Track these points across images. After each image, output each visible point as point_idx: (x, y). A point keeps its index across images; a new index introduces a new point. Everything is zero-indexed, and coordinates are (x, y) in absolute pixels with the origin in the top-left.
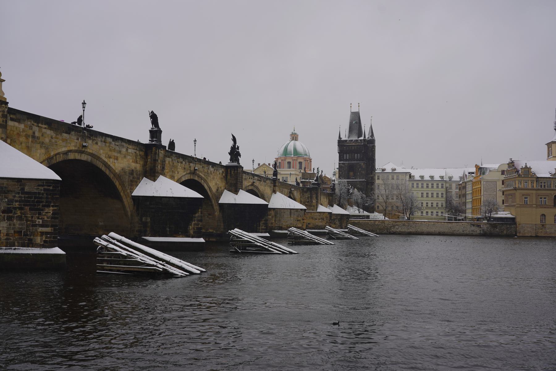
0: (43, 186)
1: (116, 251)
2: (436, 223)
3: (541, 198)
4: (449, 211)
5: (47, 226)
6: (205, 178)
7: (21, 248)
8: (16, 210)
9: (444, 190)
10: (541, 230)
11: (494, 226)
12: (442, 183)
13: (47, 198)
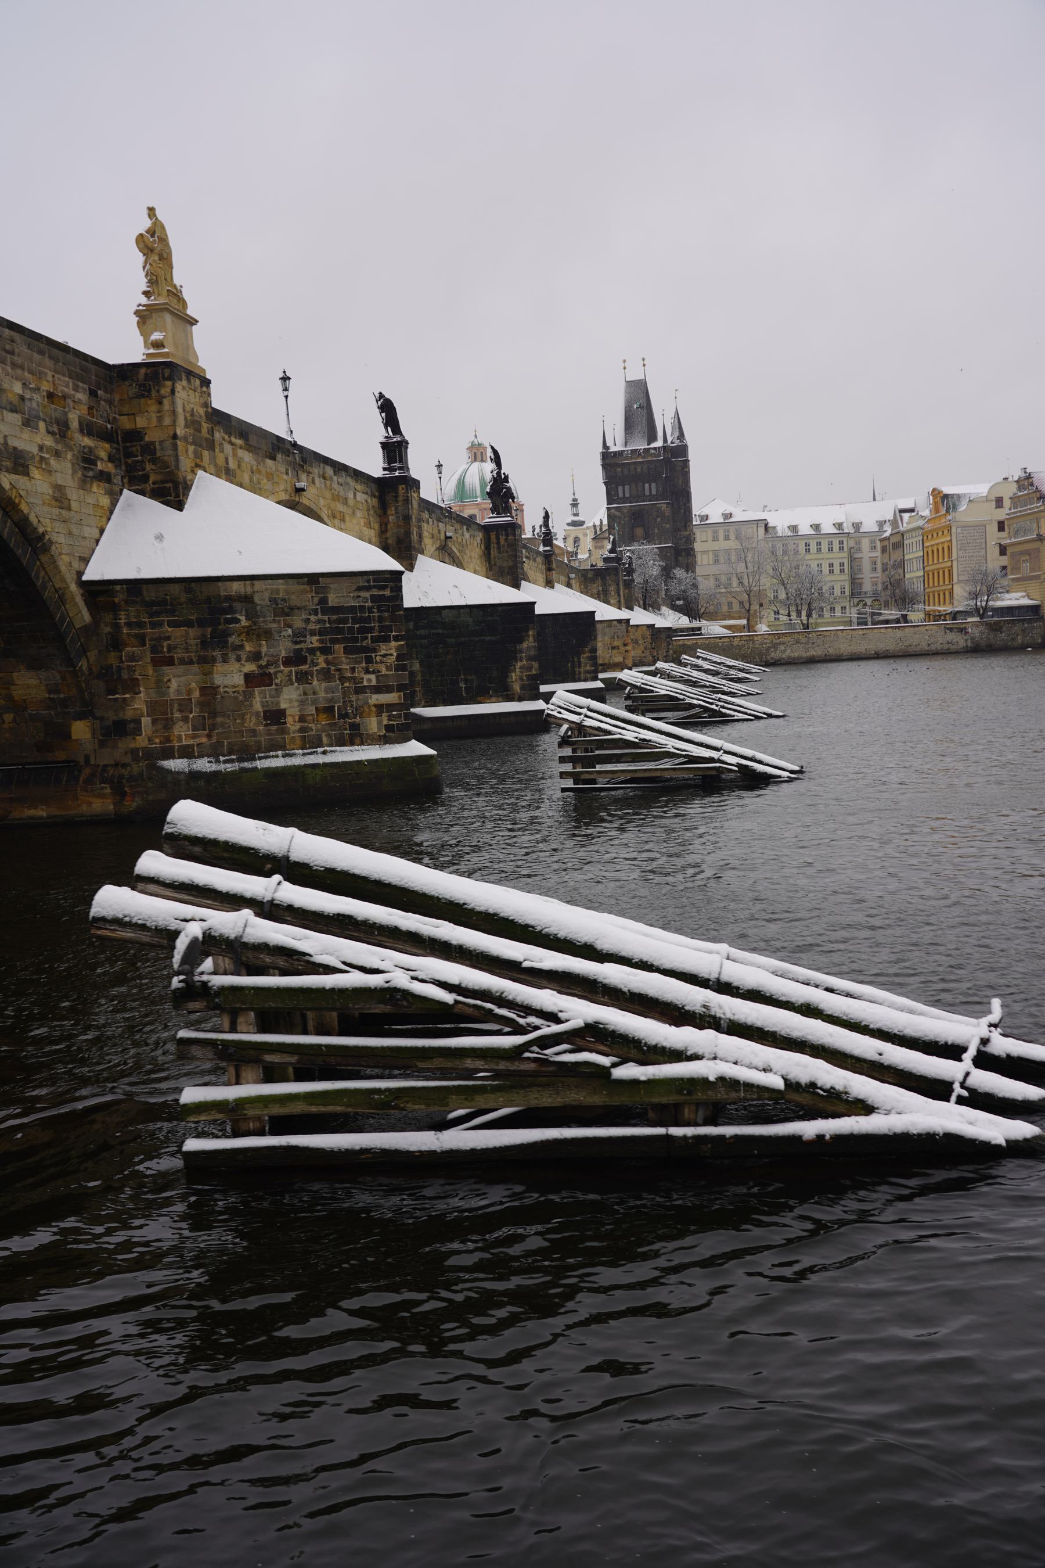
0: (367, 588)
1: (609, 733)
2: (868, 631)
5: (388, 690)
6: (460, 558)
7: (338, 748)
8: (315, 655)
9: (845, 555)
12: (841, 539)
13: (381, 619)
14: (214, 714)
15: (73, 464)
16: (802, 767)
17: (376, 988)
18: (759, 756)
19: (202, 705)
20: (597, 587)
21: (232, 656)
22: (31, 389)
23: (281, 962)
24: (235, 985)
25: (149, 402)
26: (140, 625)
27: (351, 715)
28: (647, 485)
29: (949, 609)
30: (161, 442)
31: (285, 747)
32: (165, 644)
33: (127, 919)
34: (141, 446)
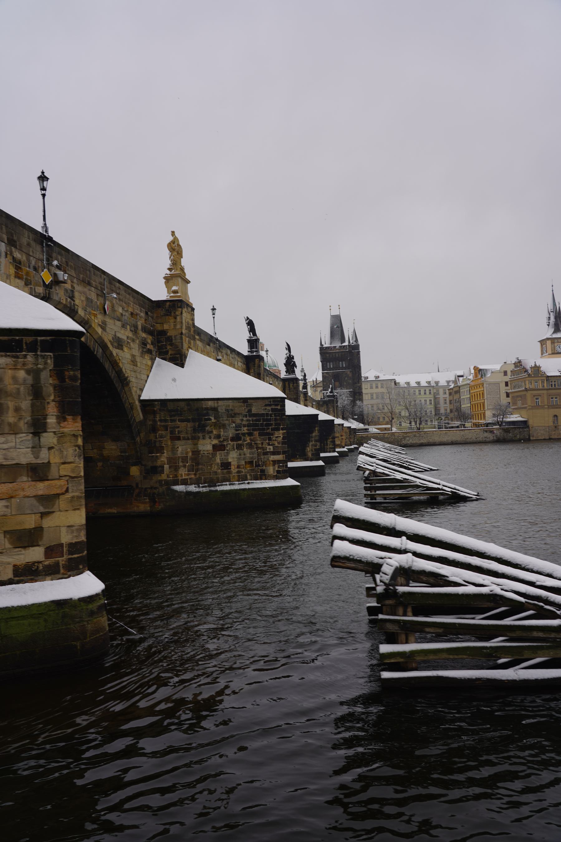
0: (270, 405)
1: (388, 475)
2: (448, 432)
3: (552, 398)
4: (438, 419)
5: (278, 453)
7: (254, 481)
8: (245, 436)
9: (432, 396)
10: (554, 432)
11: (507, 431)
13: (276, 420)
14: (198, 464)
15: (139, 345)
16: (478, 493)
17: (485, 594)
18: (457, 487)
19: (192, 459)
20: (325, 408)
21: (207, 436)
22: (125, 310)
23: (432, 580)
24: (410, 591)
25: (170, 318)
26: (166, 421)
27: (261, 466)
28: (341, 362)
29: (482, 421)
30: (175, 336)
31: (230, 480)
32: (177, 430)
33: (351, 557)
34: (165, 338)
